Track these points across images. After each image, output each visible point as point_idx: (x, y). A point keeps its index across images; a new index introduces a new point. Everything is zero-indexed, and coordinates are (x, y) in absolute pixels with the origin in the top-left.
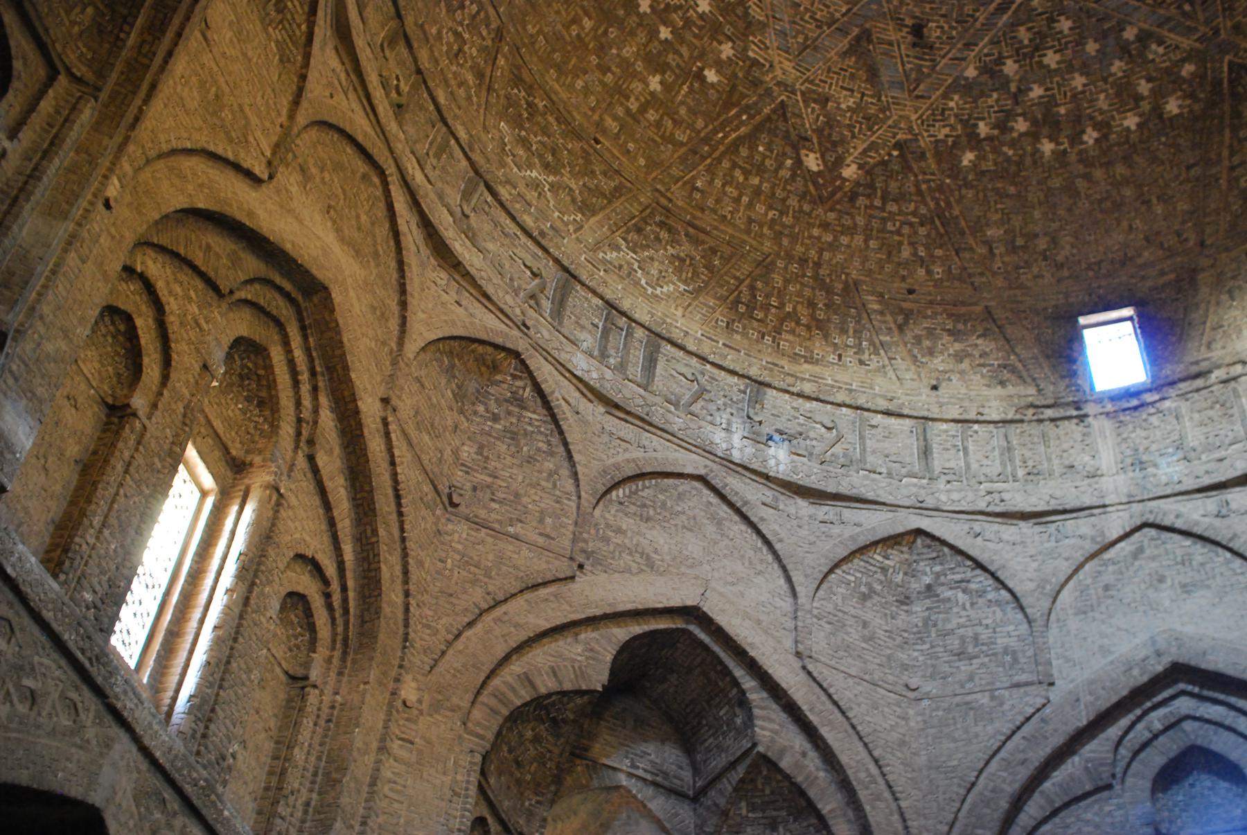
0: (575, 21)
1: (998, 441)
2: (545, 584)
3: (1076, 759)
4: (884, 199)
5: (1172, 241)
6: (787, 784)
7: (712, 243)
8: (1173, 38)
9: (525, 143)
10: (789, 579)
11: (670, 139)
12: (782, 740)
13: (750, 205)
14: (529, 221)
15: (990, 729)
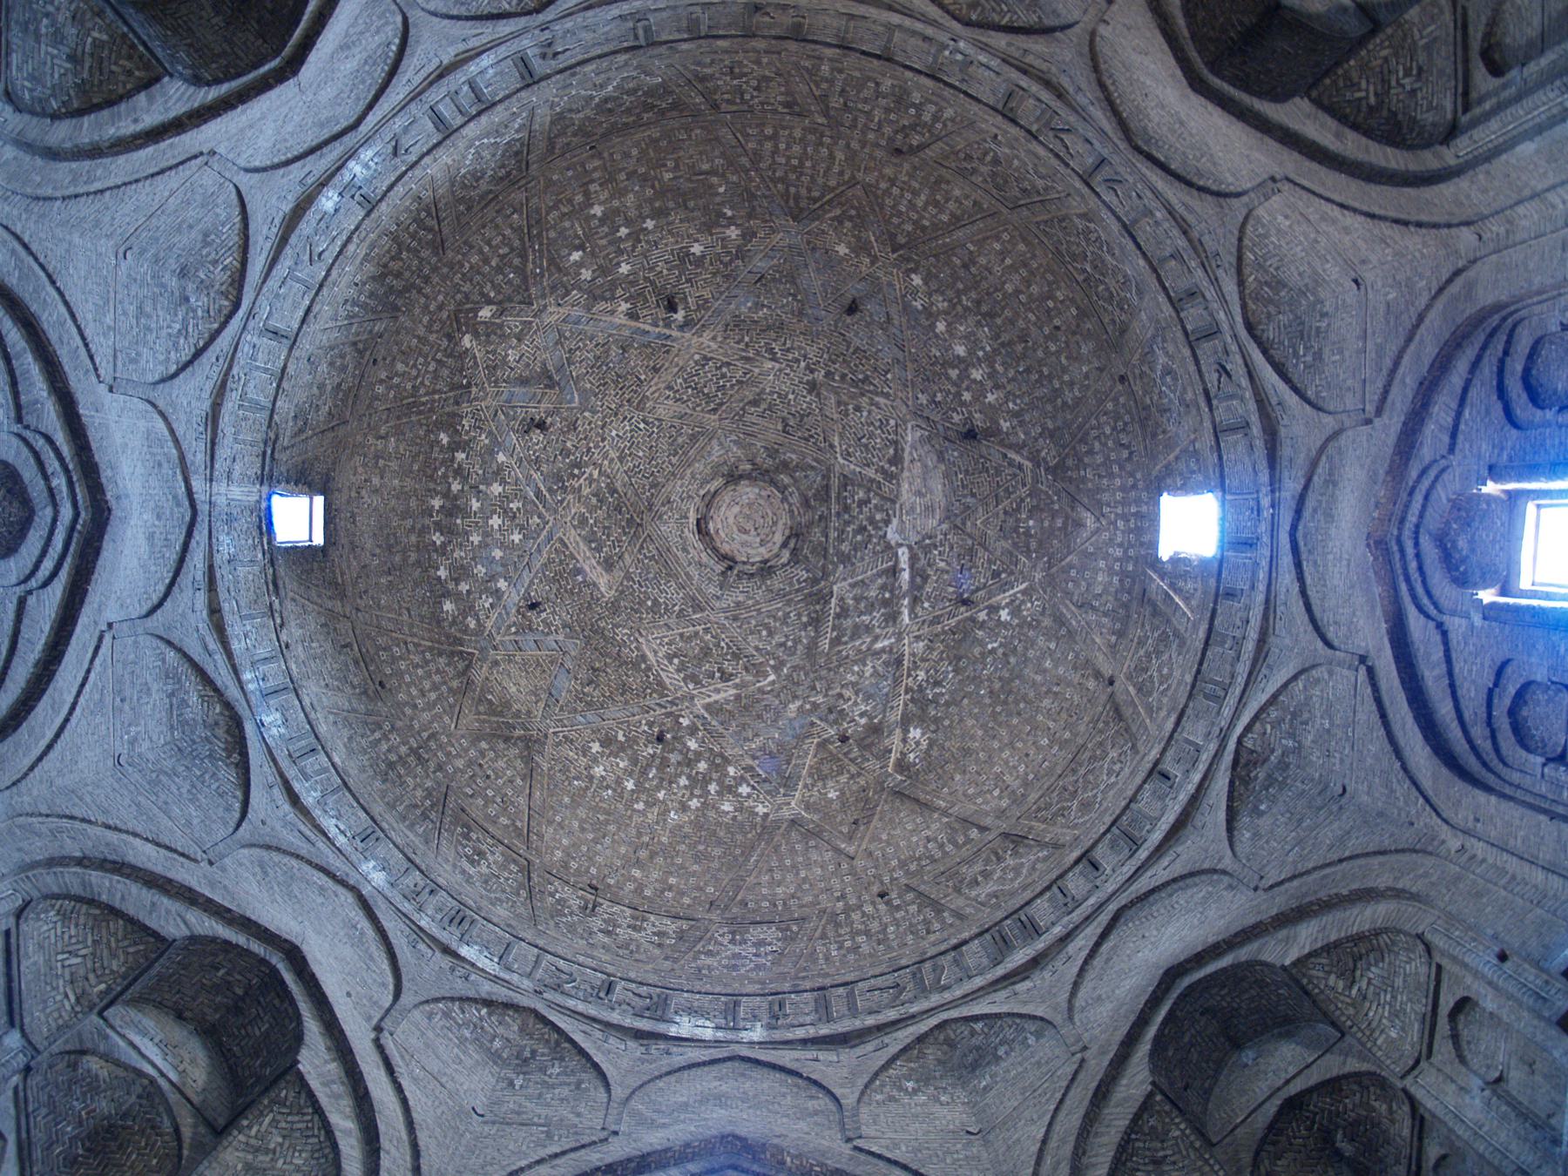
0: (677, 167)
3: (45, 394)
4: (439, 362)
6: (121, 91)
7: (475, 210)
9: (635, 91)
10: (256, 170)
11: (555, 207)
12: (158, 105)
13: (481, 252)
14: (589, 68)
15: (90, 316)
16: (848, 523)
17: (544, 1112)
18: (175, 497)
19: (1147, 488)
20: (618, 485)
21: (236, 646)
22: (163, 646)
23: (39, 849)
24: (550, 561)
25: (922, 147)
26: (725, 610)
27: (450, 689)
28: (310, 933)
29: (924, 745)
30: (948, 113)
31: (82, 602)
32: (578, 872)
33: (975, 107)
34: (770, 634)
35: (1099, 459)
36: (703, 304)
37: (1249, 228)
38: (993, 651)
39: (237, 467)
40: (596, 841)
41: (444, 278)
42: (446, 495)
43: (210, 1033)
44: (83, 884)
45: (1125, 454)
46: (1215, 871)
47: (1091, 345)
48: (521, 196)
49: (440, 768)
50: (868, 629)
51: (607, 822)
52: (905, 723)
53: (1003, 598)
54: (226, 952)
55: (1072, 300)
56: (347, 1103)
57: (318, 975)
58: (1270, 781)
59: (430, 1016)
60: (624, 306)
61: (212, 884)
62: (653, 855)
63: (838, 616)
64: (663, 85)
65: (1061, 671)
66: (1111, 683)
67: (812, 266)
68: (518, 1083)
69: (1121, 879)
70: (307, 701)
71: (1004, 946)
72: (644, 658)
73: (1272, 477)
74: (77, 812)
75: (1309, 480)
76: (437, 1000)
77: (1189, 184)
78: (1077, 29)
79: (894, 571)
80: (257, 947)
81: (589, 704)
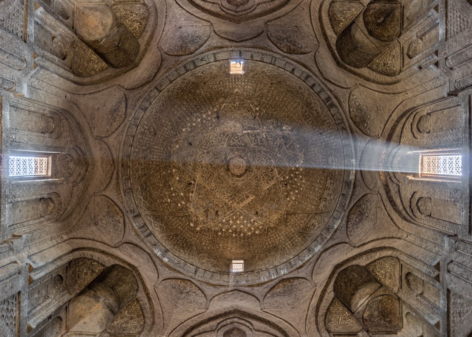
1: (211, 274)
2: (107, 245)
5: (253, 252)
8: (259, 222)
9: (142, 193)
11: (168, 210)
13: (178, 226)
14: (137, 202)
16: (238, 144)
17: (373, 209)
18: (232, 294)
19: (229, 77)
20: (230, 195)
21: (266, 280)
22: (266, 297)
23: (314, 327)
24: (247, 210)
25: (154, 129)
26: (257, 171)
27: (276, 232)
28: (332, 263)
29: (287, 126)
30: (146, 123)
31: (256, 316)
32: (317, 202)
33: (145, 117)
34: (263, 161)
35: (222, 88)
36: (190, 177)
37: (169, 53)
38: (266, 111)
39: (226, 280)
40: (309, 199)
41: (184, 234)
42: (232, 233)
43: (356, 288)
44: (321, 316)
45: (221, 82)
46: (315, 56)
47: (197, 90)
48: (166, 217)
49: (293, 234)
50: (261, 139)
51: (305, 196)
52: (282, 130)
53: (254, 109)
54: (337, 282)
55: (187, 95)
56: (373, 254)
57: (342, 261)
58: (294, 45)
59: (351, 235)
60: (190, 194)
61: (321, 286)
62: (313, 186)
63: (258, 146)
64: (140, 186)
65: (270, 95)
66: (272, 84)
67: (181, 153)
68: (367, 215)
69: (317, 79)
70: (279, 264)
71: (332, 105)
72: (268, 189)
73: (225, 47)
74: (305, 318)
75: (225, 38)
76: (347, 234)
77: (160, 67)
78: (125, 93)
79: (248, 134)
80: (336, 275)
81: (279, 200)
